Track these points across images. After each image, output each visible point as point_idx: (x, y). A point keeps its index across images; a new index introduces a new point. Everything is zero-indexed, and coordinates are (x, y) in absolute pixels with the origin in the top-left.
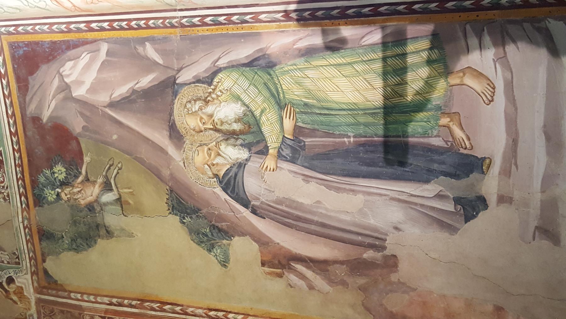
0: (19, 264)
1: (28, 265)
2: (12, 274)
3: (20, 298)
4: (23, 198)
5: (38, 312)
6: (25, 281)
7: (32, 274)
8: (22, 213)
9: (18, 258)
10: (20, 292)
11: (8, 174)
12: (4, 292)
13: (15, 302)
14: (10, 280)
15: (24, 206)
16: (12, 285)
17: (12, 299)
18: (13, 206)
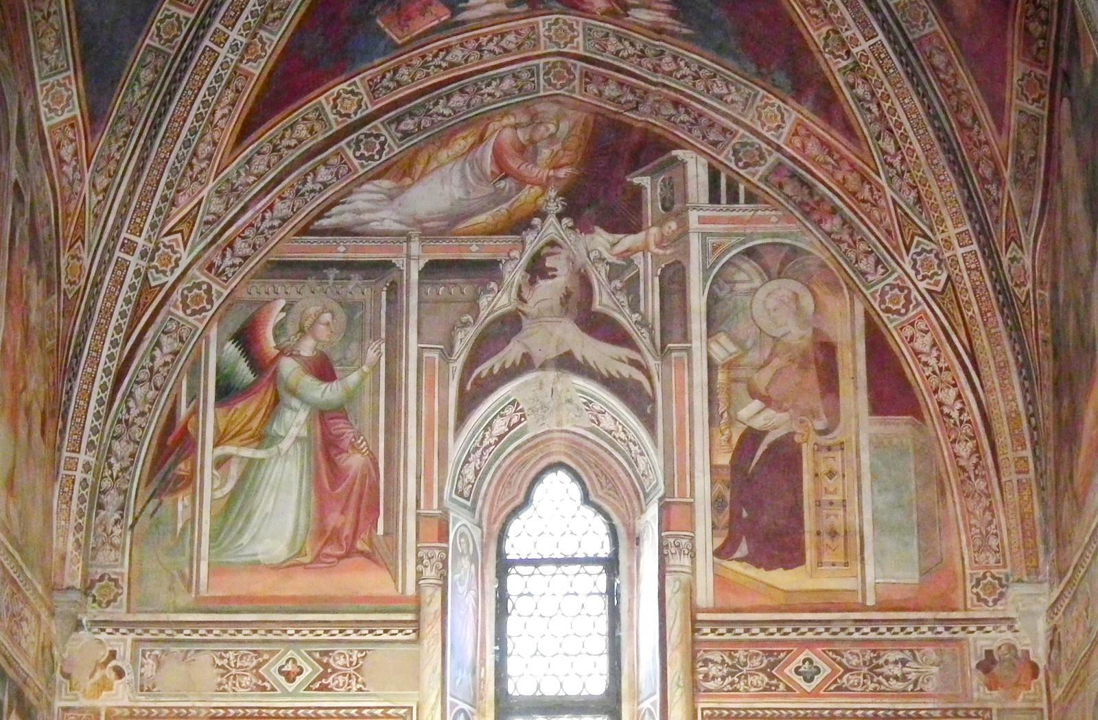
0: (142, 691)
1: (141, 704)
2: (126, 678)
3: (97, 684)
4: (222, 712)
5: (81, 710)
6: (120, 696)
7: (130, 708)
8: (206, 708)
9: (149, 690)
10: (104, 686)
11: (250, 695)
12: (103, 660)
13: (92, 676)
14: (120, 673)
15: (213, 711)
16: (111, 675)
17: (95, 671)
18: (213, 696)
